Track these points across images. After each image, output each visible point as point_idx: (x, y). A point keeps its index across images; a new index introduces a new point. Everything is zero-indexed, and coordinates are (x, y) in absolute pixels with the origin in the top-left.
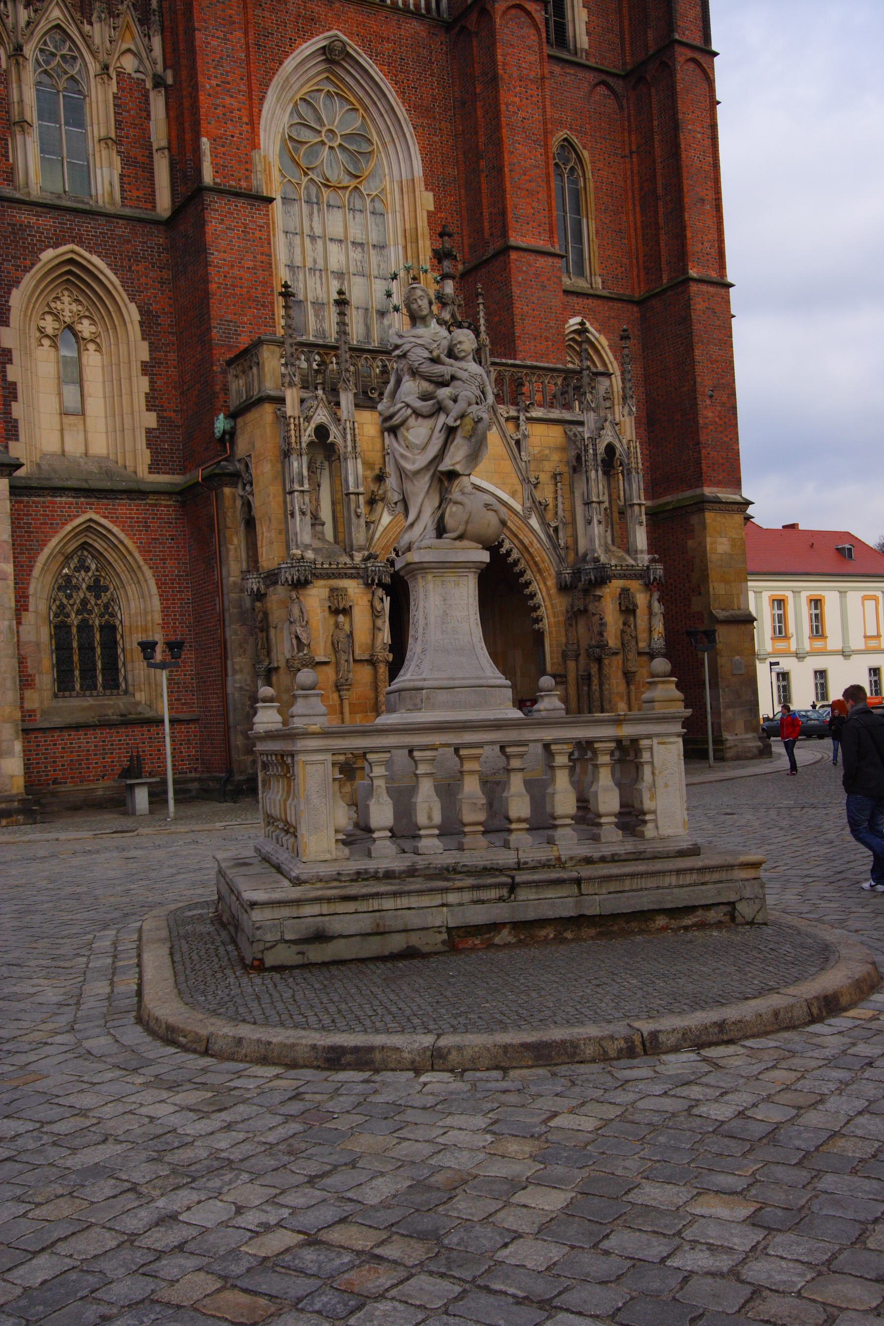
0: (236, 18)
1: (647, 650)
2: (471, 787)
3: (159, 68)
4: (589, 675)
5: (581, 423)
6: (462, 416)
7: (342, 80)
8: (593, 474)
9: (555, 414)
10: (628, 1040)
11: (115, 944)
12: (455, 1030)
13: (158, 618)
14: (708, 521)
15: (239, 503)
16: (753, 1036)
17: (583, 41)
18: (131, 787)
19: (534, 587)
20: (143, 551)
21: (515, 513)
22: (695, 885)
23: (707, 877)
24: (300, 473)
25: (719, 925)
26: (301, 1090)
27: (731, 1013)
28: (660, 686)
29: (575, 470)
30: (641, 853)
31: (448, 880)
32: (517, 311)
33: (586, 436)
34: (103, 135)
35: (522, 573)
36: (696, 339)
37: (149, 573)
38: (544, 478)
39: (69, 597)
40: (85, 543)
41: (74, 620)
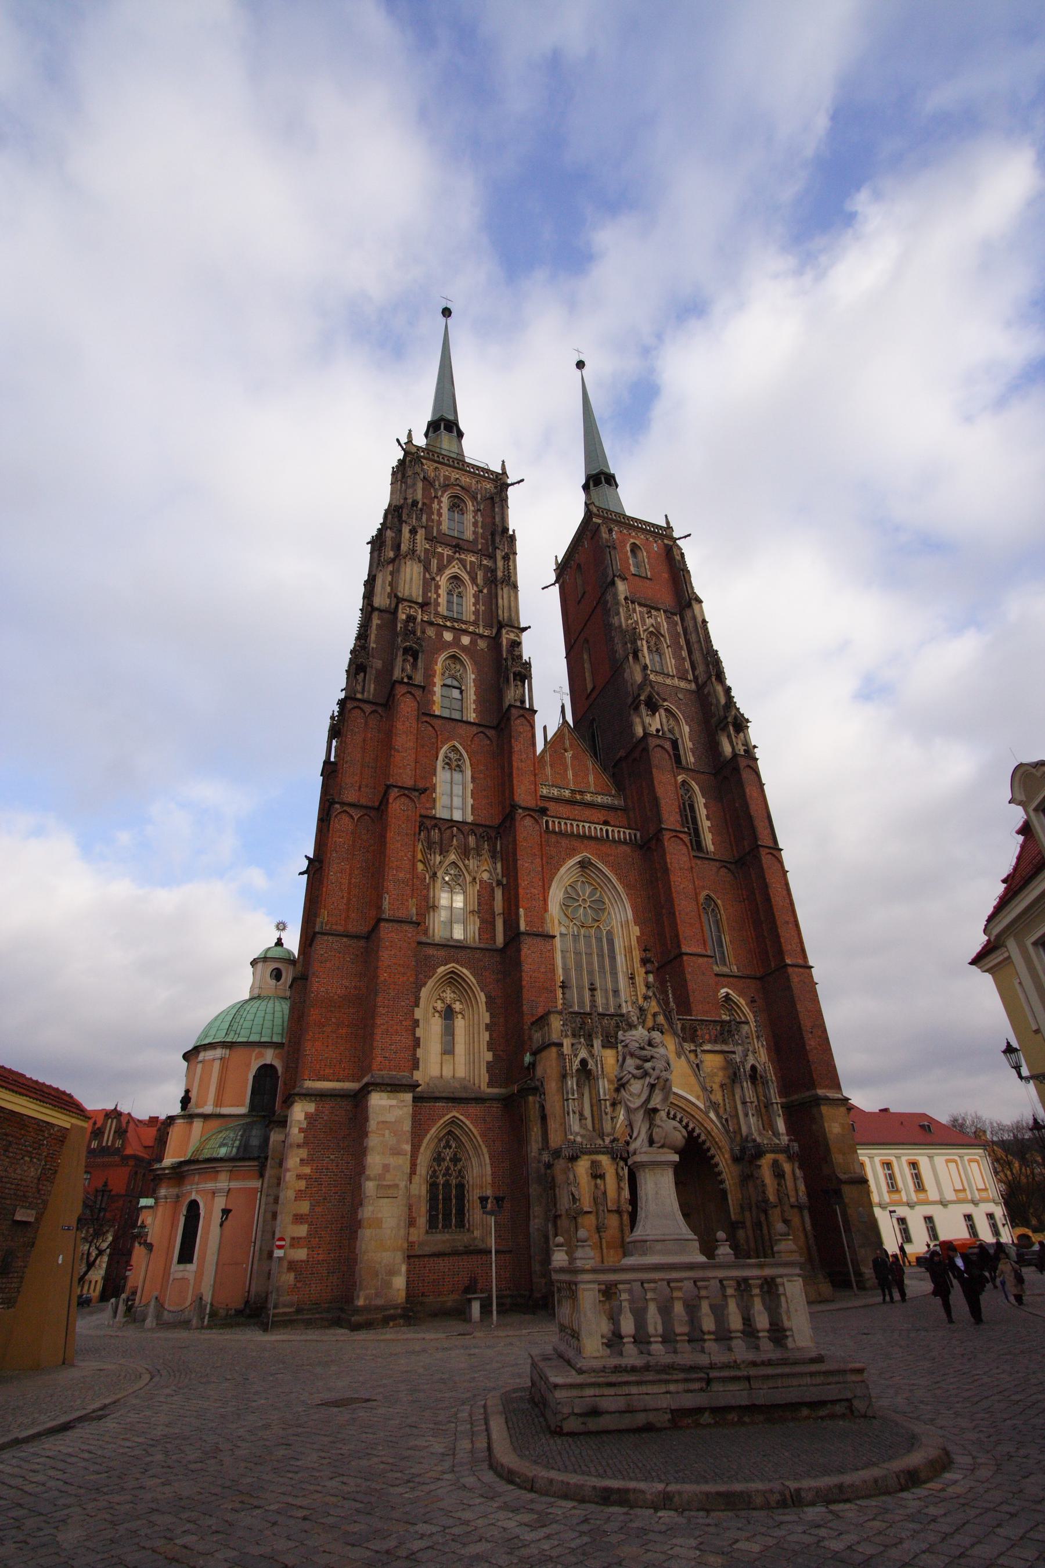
0: (537, 853)
1: (796, 1204)
2: (678, 1308)
3: (500, 877)
4: (760, 1222)
5: (734, 1052)
6: (658, 1078)
7: (589, 875)
8: (745, 1084)
9: (718, 1047)
10: (782, 1494)
11: (470, 1415)
12: (677, 1482)
13: (489, 1179)
14: (823, 1112)
15: (537, 1106)
16: (863, 1498)
17: (711, 848)
18: (470, 1301)
19: (717, 1159)
20: (483, 1135)
21: (701, 1110)
22: (823, 1384)
23: (831, 1379)
24: (572, 1088)
25: (843, 1416)
26: (588, 1517)
27: (847, 1479)
28: (783, 1242)
29: (734, 1081)
30: (786, 1359)
31: (669, 1374)
32: (689, 988)
33: (738, 1060)
34: (472, 909)
35: (709, 1149)
36: (796, 999)
37: (485, 1150)
38: (716, 1087)
39: (439, 1165)
41: (441, 1180)
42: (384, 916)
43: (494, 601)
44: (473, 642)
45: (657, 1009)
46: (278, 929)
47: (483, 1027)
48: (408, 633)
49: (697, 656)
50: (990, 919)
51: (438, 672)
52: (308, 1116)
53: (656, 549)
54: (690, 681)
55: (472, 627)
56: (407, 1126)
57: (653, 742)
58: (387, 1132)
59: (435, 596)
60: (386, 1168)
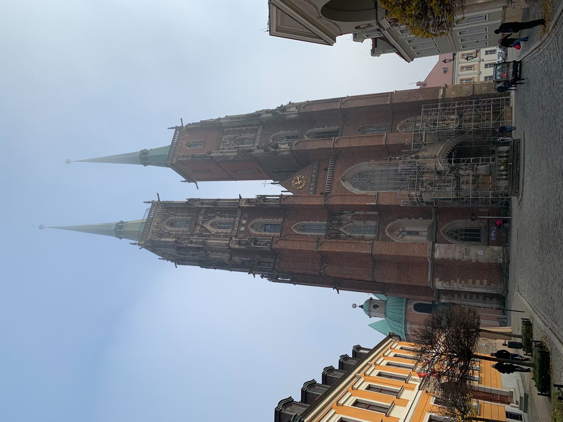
3: (350, 212)
39: (458, 238)
40: (447, 233)
41: (463, 237)
42: (370, 252)
43: (223, 209)
44: (244, 219)
45: (409, 157)
46: (355, 307)
47: (409, 220)
48: (247, 244)
50: (406, 60)
51: (260, 233)
52: (440, 280)
53: (188, 135)
54: (258, 127)
55: (237, 219)
56: (447, 245)
57: (294, 148)
58: (448, 252)
59: (222, 234)
60: (460, 252)
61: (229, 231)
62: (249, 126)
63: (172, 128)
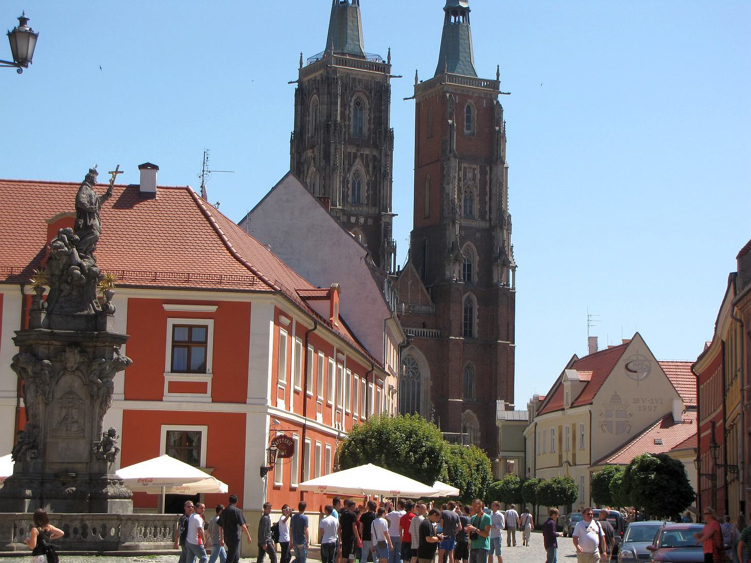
43: (378, 186)
44: (366, 221)
49: (493, 204)
53: (484, 105)
59: (346, 190)
61: (350, 199)
62: (490, 207)
63: (498, 75)
